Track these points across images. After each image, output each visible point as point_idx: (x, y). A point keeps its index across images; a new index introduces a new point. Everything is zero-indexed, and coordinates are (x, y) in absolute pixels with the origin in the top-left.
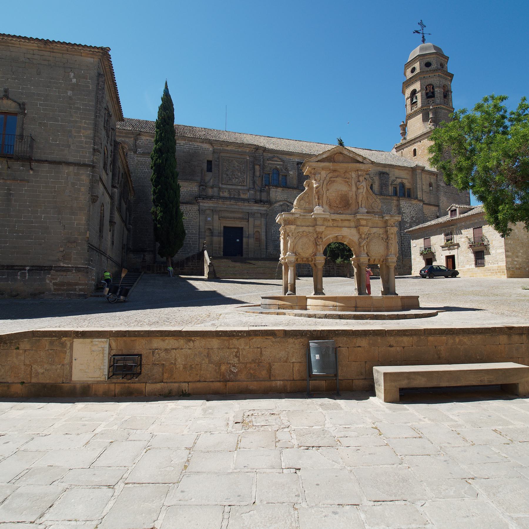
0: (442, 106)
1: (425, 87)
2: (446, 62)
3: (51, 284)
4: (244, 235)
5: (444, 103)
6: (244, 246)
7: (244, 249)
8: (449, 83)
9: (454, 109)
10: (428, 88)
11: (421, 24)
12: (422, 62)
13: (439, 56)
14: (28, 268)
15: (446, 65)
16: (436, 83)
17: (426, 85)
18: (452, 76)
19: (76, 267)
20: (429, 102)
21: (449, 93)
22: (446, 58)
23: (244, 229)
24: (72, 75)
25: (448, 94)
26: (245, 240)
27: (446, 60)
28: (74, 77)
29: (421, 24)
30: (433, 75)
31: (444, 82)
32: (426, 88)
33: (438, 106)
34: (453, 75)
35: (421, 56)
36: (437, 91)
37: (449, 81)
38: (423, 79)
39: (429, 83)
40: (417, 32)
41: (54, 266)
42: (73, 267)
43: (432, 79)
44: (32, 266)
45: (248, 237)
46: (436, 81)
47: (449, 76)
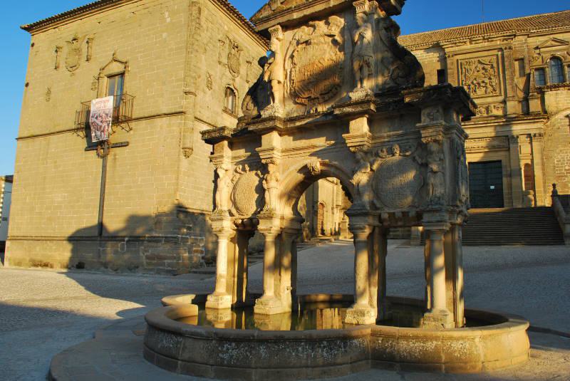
3: (144, 257)
4: (504, 173)
6: (505, 191)
7: (504, 194)
14: (126, 239)
19: (166, 237)
23: (504, 163)
24: (167, 14)
26: (505, 180)
28: (169, 16)
41: (147, 235)
42: (162, 237)
44: (130, 237)
45: (510, 176)
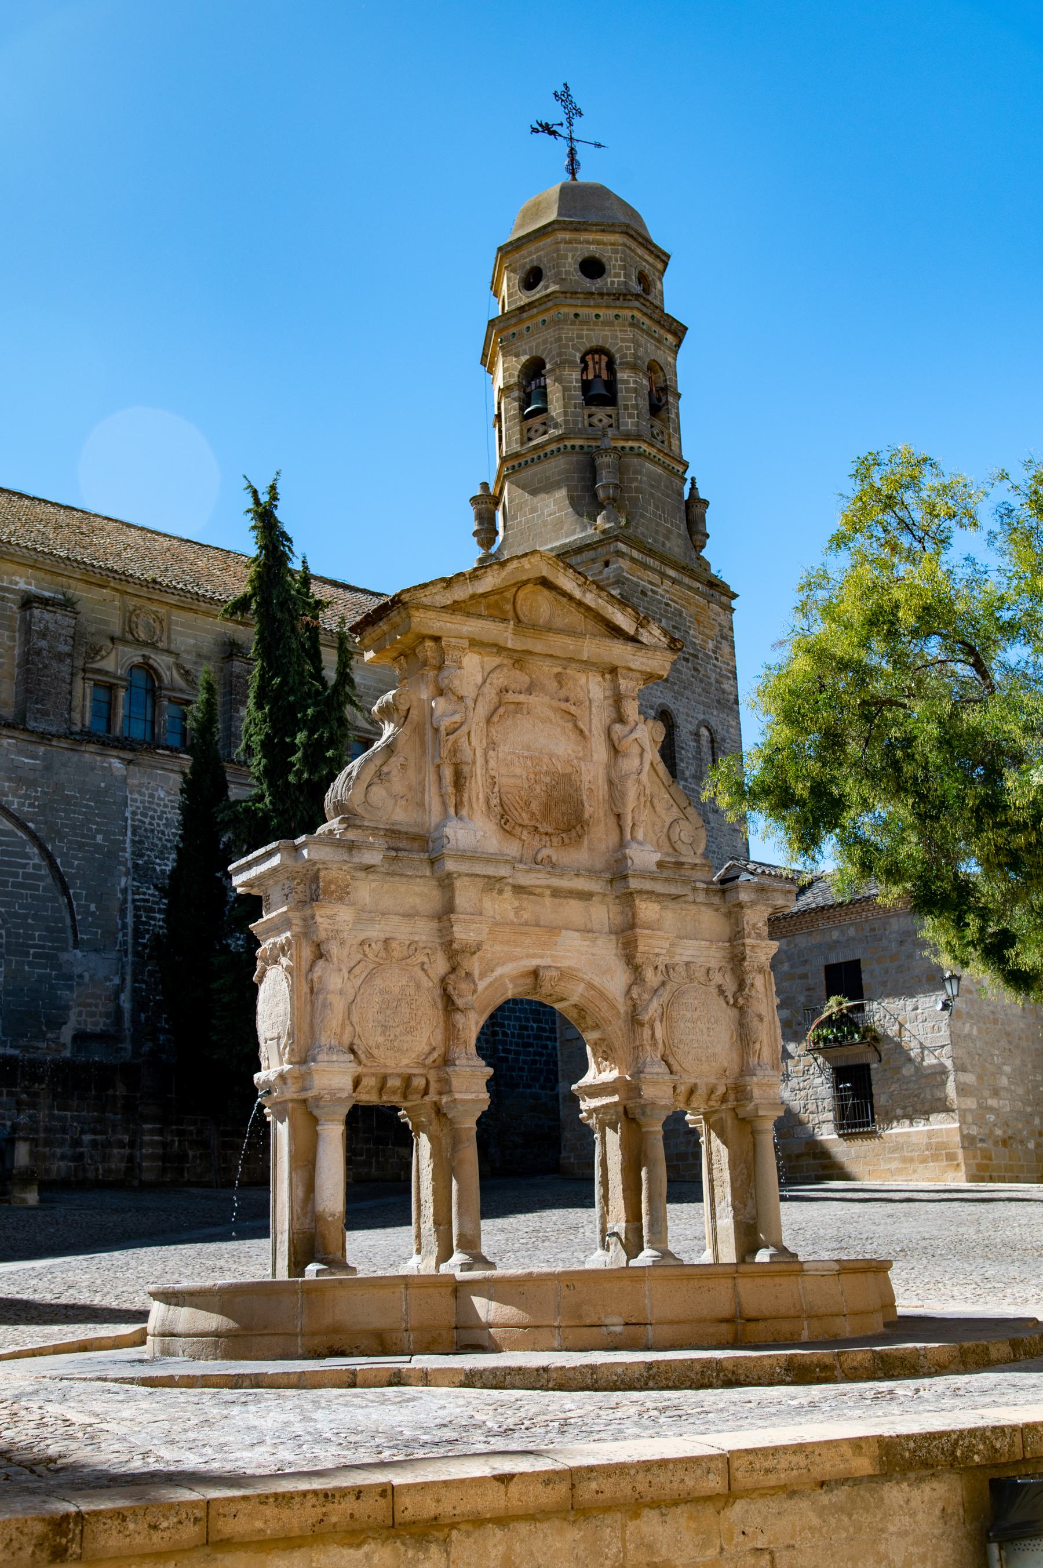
0: (644, 447)
1: (578, 355)
2: (657, 274)
5: (653, 436)
8: (670, 359)
9: (686, 465)
10: (591, 364)
11: (564, 97)
12: (570, 255)
13: (633, 245)
15: (658, 283)
16: (621, 349)
17: (583, 350)
18: (679, 331)
20: (595, 420)
21: (671, 399)
22: (658, 257)
25: (667, 401)
27: (660, 266)
29: (564, 97)
30: (612, 312)
31: (650, 351)
32: (583, 360)
33: (630, 444)
34: (686, 329)
35: (565, 229)
36: (627, 382)
37: (670, 349)
38: (573, 323)
39: (594, 344)
40: (548, 129)
43: (607, 332)
46: (623, 340)
47: (669, 331)
